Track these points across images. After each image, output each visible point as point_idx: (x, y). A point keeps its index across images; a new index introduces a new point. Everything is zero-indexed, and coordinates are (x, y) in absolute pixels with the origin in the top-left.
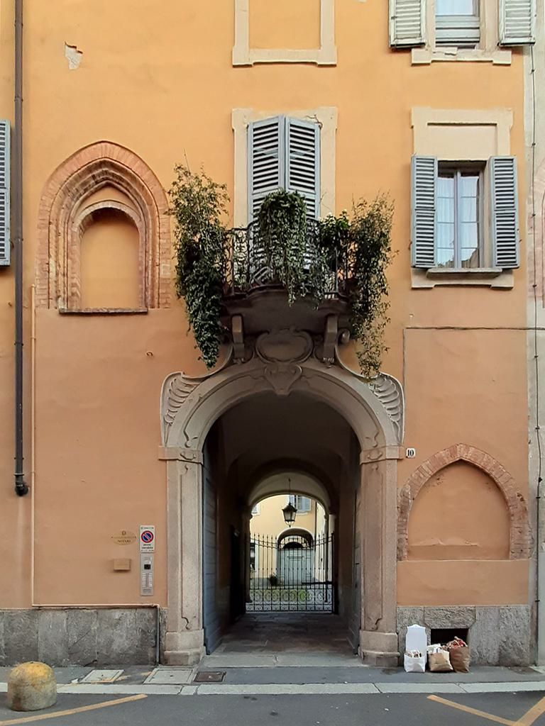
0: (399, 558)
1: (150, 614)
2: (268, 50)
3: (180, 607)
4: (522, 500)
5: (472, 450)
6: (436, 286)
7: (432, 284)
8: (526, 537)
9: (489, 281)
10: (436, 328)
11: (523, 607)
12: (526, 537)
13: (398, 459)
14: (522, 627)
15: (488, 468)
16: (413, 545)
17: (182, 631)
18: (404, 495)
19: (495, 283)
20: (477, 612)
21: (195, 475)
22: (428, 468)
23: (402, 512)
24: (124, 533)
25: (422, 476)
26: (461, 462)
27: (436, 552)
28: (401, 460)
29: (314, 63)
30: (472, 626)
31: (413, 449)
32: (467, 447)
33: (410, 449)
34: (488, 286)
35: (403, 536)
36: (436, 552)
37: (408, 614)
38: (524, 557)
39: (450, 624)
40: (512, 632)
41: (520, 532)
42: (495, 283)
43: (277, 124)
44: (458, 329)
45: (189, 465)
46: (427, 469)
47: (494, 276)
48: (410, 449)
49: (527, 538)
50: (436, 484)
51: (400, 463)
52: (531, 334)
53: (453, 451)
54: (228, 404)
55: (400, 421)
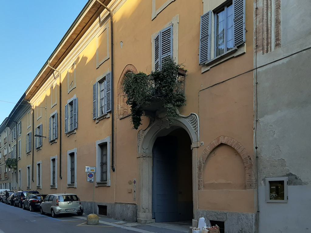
0: (199, 189)
1: (134, 206)
2: (160, 8)
3: (141, 204)
4: (250, 159)
5: (226, 138)
6: (211, 68)
7: (208, 68)
8: (253, 178)
9: (233, 55)
10: (211, 87)
11: (250, 214)
12: (253, 178)
13: (197, 147)
14: (249, 224)
15: (233, 145)
16: (205, 183)
17: (142, 212)
18: (200, 162)
19: (235, 55)
20: (228, 214)
21: (147, 162)
22: (209, 150)
23: (199, 169)
24: (130, 181)
25: (206, 153)
26: (222, 144)
27: (213, 186)
28: (199, 147)
29: (172, 2)
30: (225, 221)
31: (203, 142)
32: (224, 137)
33: (201, 142)
34: (233, 57)
35: (200, 179)
36: (213, 186)
37: (201, 213)
38: (252, 189)
39: (217, 219)
40: (244, 226)
41: (249, 176)
42: (235, 55)
43: (170, 29)
44: (220, 83)
45: (144, 158)
46: (208, 149)
47: (235, 51)
48: (201, 142)
49: (253, 178)
50: (213, 156)
51: (198, 148)
52: (255, 71)
53: (218, 139)
54: (155, 136)
55: (197, 131)
